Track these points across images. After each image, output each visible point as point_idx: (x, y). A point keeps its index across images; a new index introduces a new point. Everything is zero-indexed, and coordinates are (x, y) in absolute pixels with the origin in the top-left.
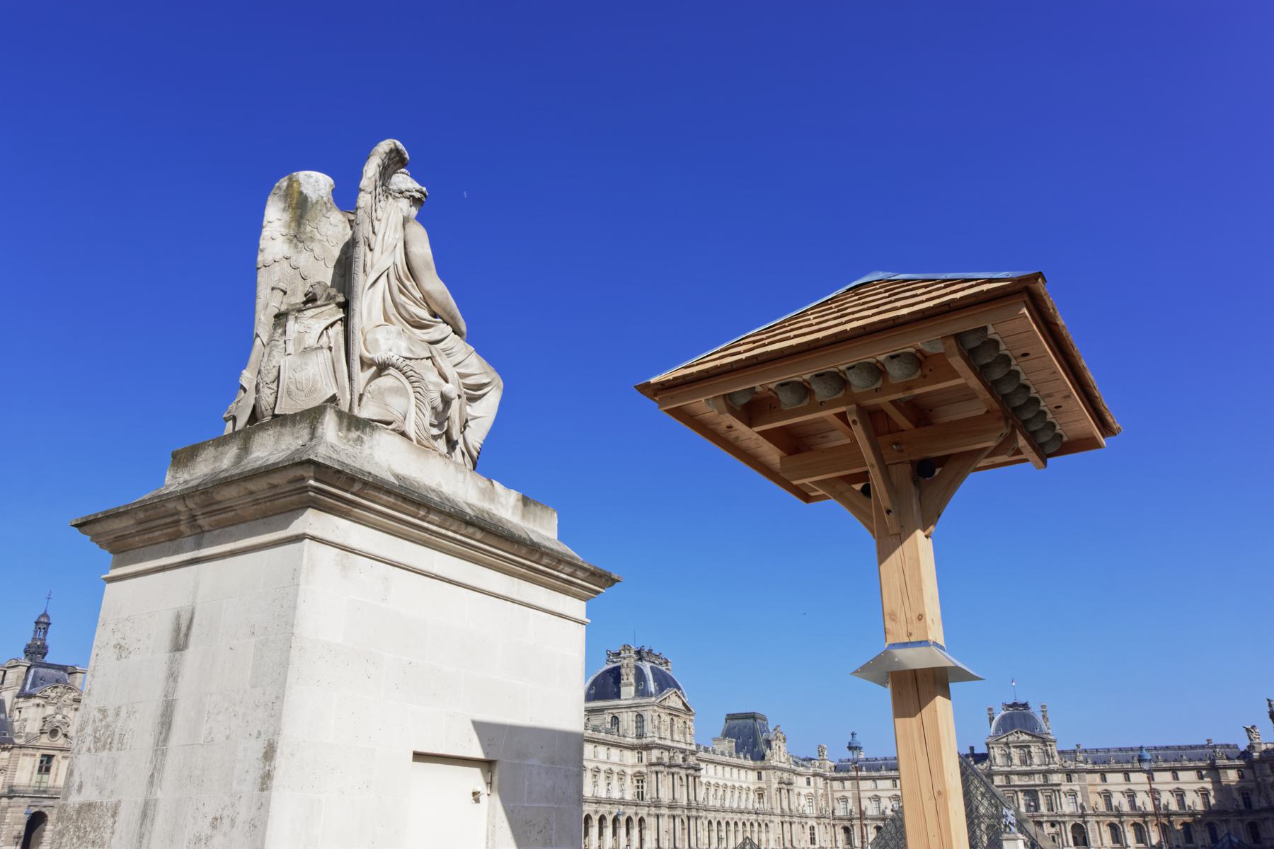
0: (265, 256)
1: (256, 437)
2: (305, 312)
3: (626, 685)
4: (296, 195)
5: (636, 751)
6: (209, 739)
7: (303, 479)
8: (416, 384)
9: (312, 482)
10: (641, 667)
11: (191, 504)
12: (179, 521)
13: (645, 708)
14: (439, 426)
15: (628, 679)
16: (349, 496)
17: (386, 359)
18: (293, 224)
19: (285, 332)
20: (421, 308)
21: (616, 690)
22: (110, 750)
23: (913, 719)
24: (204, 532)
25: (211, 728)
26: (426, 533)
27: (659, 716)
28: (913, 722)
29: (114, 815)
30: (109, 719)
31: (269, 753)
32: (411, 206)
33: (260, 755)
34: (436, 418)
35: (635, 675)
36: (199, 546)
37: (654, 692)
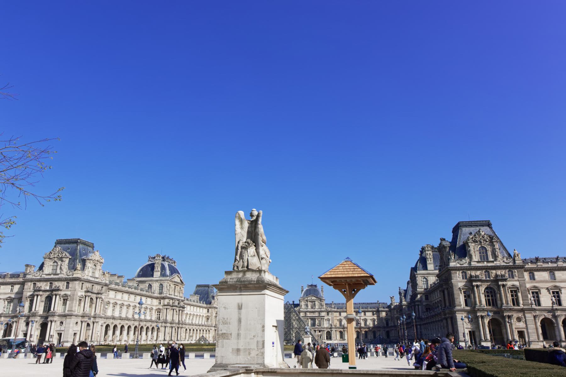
1: (247, 273)
3: (156, 271)
5: (158, 300)
7: (266, 286)
10: (164, 264)
11: (241, 286)
13: (164, 282)
15: (157, 269)
19: (247, 252)
21: (151, 273)
27: (180, 288)
29: (231, 335)
31: (263, 327)
33: (262, 327)
35: (161, 267)
36: (241, 292)
37: (168, 275)
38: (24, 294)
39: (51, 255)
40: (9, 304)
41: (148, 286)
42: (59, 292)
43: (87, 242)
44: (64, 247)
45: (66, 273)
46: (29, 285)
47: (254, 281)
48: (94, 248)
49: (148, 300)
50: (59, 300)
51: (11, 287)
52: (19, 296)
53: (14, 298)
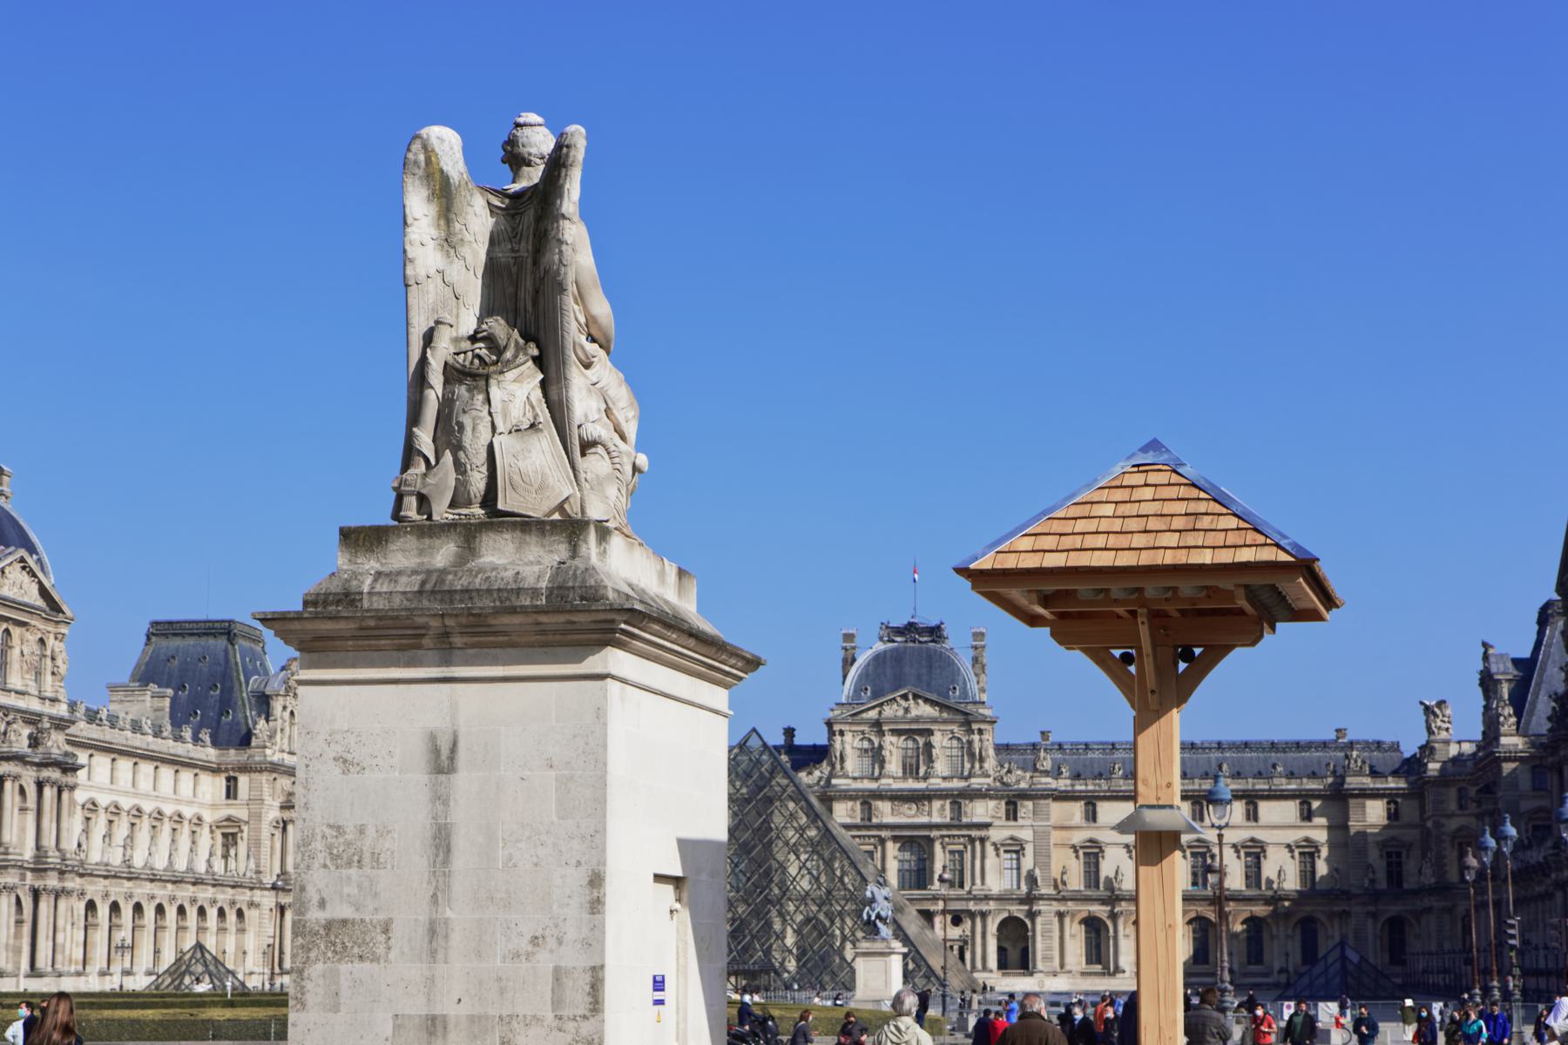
0: (418, 270)
1: (484, 538)
4: (437, 176)
6: (510, 865)
7: (613, 621)
11: (450, 622)
12: (424, 635)
18: (442, 222)
19: (488, 401)
22: (360, 867)
23: (1155, 868)
24: (452, 648)
25: (511, 854)
27: (42, 641)
28: (1155, 870)
29: (386, 931)
31: (596, 880)
33: (585, 882)
36: (447, 662)
47: (535, 592)
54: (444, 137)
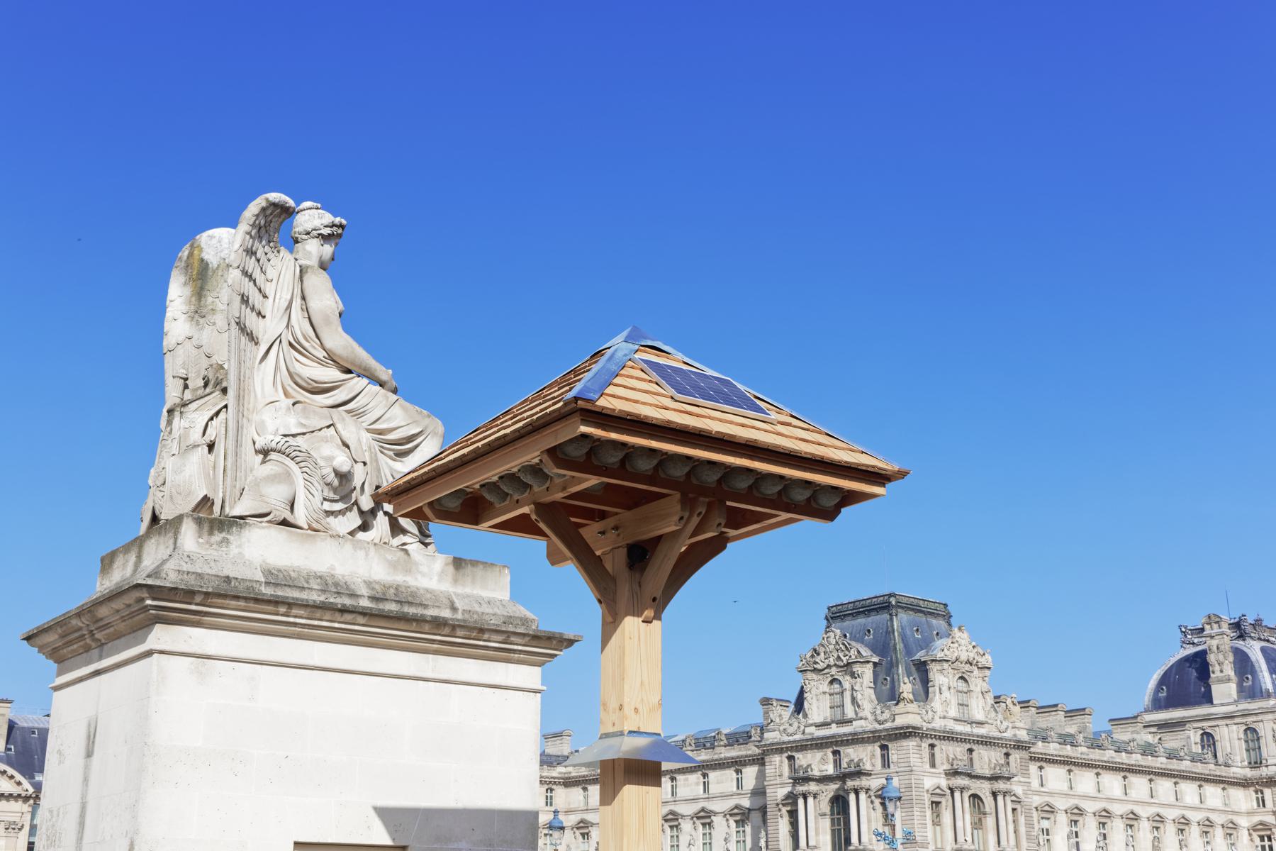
2: (189, 406)
3: (1220, 681)
4: (196, 264)
5: (1252, 789)
8: (302, 465)
9: (149, 602)
10: (1245, 649)
13: (1260, 717)
14: (344, 498)
15: (1221, 671)
16: (193, 607)
17: (264, 446)
18: (193, 299)
20: (328, 367)
21: (1203, 689)
23: (609, 807)
24: (103, 644)
26: (295, 627)
30: (54, 819)
32: (322, 245)
34: (335, 493)
35: (1234, 663)
37: (1271, 690)
38: (768, 795)
39: (817, 660)
40: (741, 829)
41: (1202, 740)
42: (863, 782)
43: (921, 602)
44: (853, 626)
45: (874, 713)
46: (777, 763)
48: (952, 620)
49: (1208, 794)
50: (868, 807)
51: (734, 774)
52: (759, 802)
53: (749, 810)
54: (215, 235)
